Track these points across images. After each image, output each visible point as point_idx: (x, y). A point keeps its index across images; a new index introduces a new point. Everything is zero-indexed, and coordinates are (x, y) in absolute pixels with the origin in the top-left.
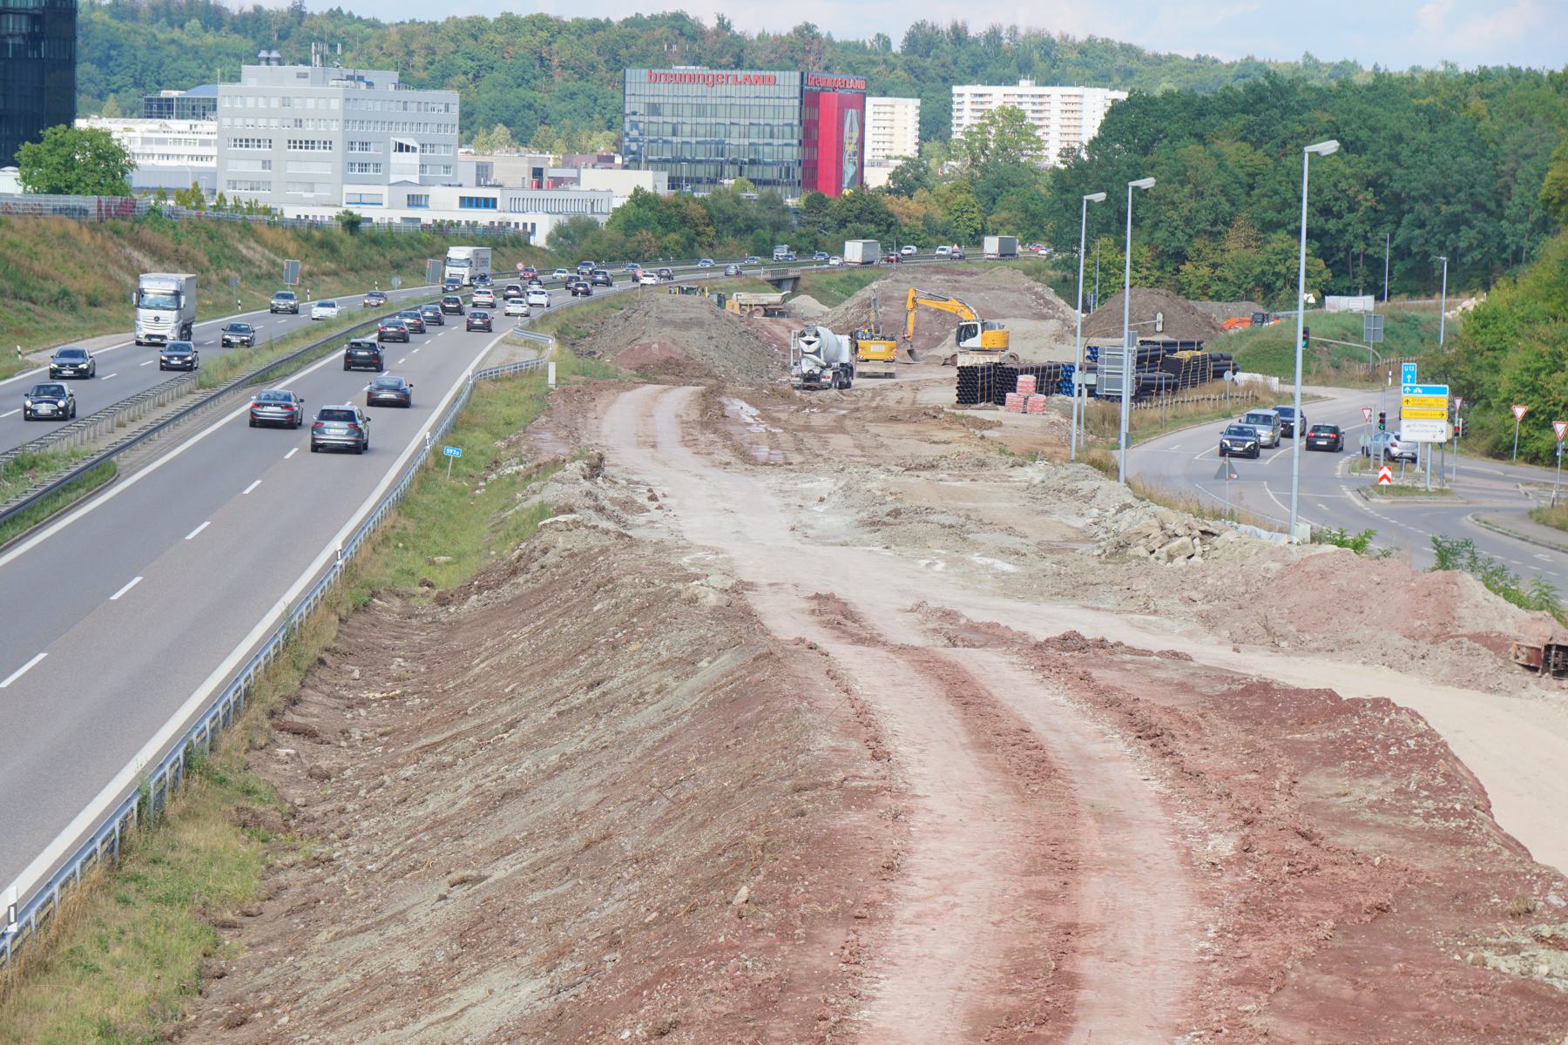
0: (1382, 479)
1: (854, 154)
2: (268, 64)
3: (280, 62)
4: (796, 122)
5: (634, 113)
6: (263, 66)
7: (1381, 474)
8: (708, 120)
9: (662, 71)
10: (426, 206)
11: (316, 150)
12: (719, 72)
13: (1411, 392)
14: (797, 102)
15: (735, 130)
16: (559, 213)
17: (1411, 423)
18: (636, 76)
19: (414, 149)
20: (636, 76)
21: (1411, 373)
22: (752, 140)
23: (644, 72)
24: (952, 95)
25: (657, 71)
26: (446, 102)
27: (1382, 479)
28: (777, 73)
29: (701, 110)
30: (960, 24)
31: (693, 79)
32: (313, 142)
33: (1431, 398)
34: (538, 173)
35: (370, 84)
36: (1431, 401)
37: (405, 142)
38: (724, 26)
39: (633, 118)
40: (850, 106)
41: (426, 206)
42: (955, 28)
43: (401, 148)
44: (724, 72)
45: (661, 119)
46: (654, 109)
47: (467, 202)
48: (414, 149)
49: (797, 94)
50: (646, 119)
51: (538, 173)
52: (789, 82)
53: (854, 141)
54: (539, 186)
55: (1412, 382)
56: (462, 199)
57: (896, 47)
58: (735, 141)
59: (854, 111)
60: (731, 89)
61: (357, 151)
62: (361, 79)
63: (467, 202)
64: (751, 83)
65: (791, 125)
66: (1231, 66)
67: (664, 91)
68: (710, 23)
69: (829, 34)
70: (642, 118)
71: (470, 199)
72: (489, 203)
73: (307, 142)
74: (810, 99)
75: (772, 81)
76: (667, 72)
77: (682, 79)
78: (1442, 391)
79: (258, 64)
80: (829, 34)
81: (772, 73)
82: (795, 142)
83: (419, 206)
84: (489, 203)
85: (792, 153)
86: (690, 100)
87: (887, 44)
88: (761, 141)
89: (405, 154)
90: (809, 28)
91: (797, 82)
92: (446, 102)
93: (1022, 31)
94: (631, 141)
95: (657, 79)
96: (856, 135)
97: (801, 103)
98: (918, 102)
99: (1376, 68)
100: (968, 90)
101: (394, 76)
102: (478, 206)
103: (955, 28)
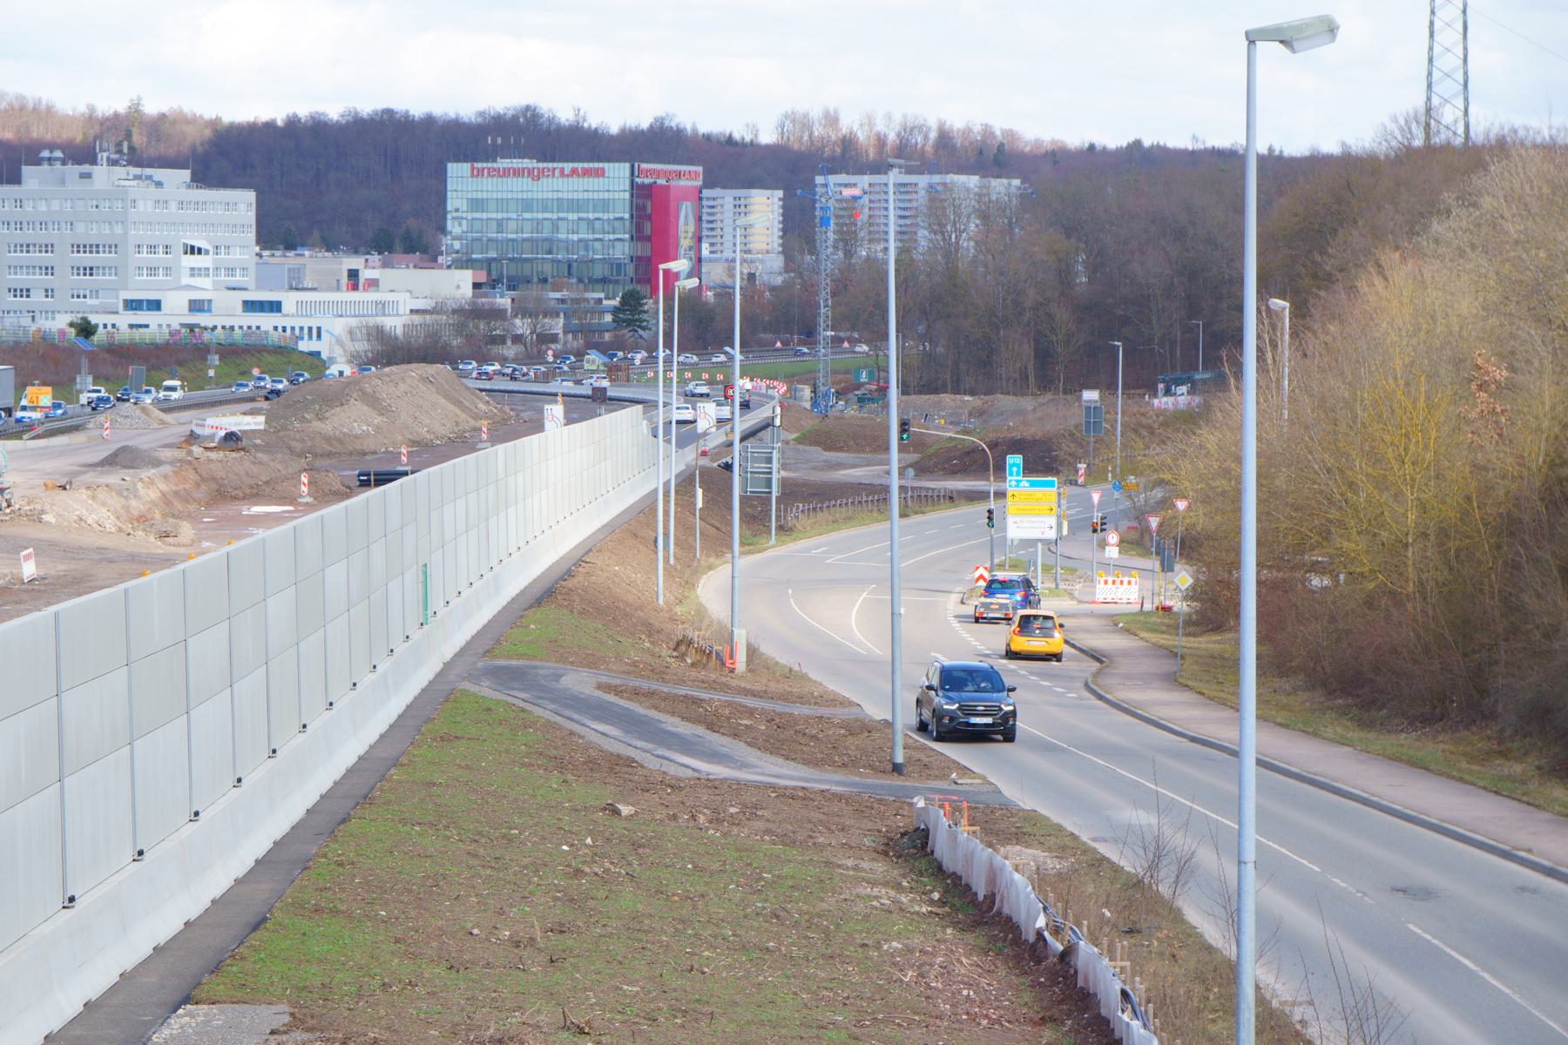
0: (977, 580)
1: (690, 248)
2: (50, 165)
3: (64, 163)
4: (627, 216)
5: (457, 210)
6: (45, 167)
7: (977, 574)
8: (535, 215)
9: (485, 165)
10: (209, 310)
11: (101, 255)
12: (545, 165)
13: (1017, 486)
14: (627, 195)
15: (562, 225)
16: (359, 316)
17: (1018, 519)
18: (457, 172)
19: (207, 252)
20: (457, 172)
21: (1014, 465)
22: (581, 236)
23: (466, 166)
24: (816, 186)
25: (479, 165)
26: (241, 204)
27: (977, 580)
28: (606, 165)
29: (527, 205)
30: (832, 112)
31: (518, 173)
32: (97, 246)
33: (1039, 492)
34: (353, 274)
35: (159, 184)
36: (1039, 495)
37: (197, 244)
39: (455, 214)
40: (686, 199)
41: (209, 310)
42: (827, 115)
43: (192, 250)
44: (550, 165)
45: (484, 216)
46: (476, 204)
47: (250, 306)
48: (207, 252)
49: (627, 187)
50: (470, 216)
51: (353, 274)
53: (690, 235)
54: (355, 287)
55: (1018, 475)
56: (246, 303)
58: (562, 236)
59: (689, 204)
61: (145, 255)
62: (149, 178)
63: (250, 306)
64: (578, 176)
65: (622, 219)
67: (489, 187)
69: (694, 124)
70: (464, 215)
71: (253, 303)
72: (275, 307)
73: (91, 246)
75: (600, 173)
76: (490, 165)
77: (506, 173)
78: (1051, 484)
79: (39, 164)
80: (694, 124)
81: (601, 165)
82: (627, 236)
83: (201, 310)
84: (275, 307)
85: (622, 251)
86: (515, 196)
88: (591, 237)
89: (196, 257)
91: (627, 174)
92: (241, 204)
94: (454, 239)
95: (480, 172)
96: (691, 228)
97: (632, 196)
98: (780, 193)
99: (1271, 150)
101: (186, 174)
102: (262, 310)
103: (827, 115)
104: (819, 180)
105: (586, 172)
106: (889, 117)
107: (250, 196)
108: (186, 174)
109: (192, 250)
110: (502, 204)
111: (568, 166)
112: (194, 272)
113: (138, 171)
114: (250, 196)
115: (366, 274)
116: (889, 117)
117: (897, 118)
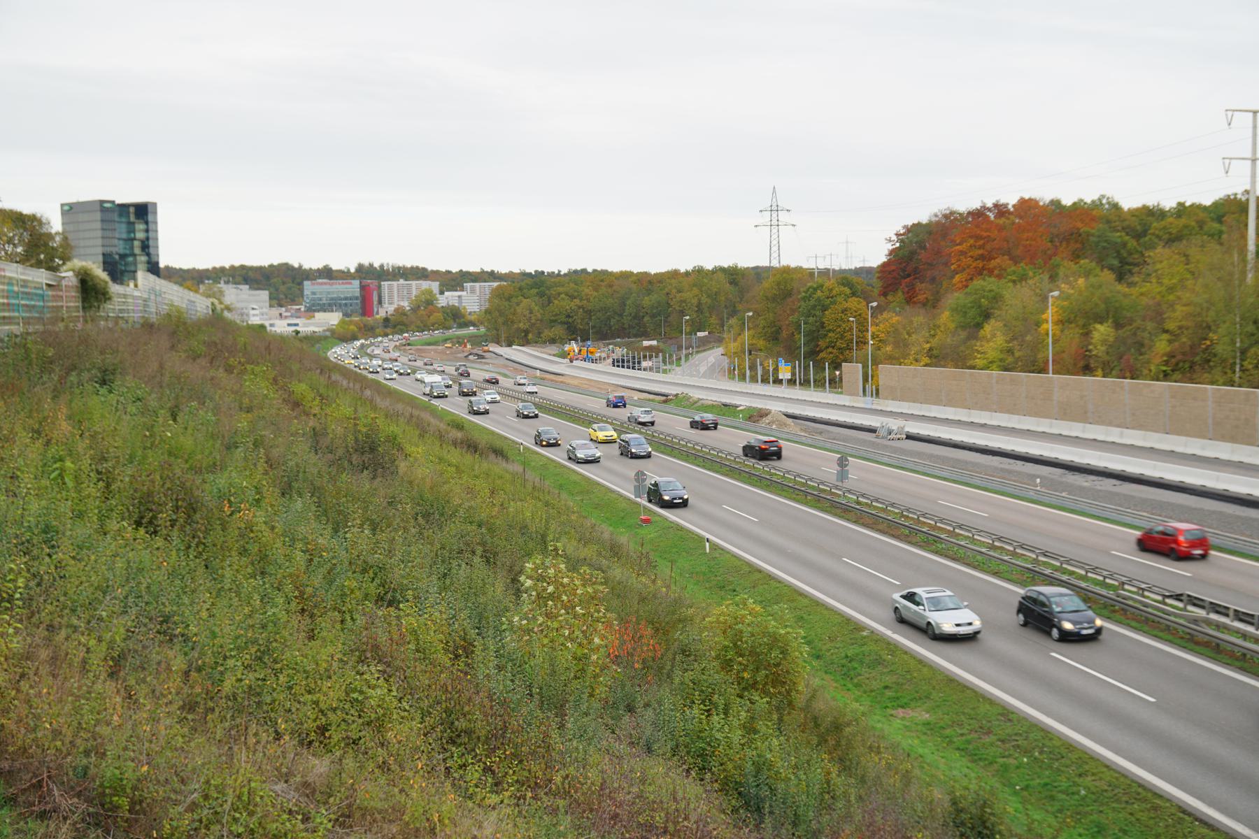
18: (307, 284)
20: (307, 284)
26: (264, 295)
29: (329, 293)
31: (325, 284)
34: (281, 314)
38: (300, 267)
43: (253, 309)
46: (314, 293)
51: (281, 314)
52: (356, 283)
57: (353, 270)
60: (338, 286)
66: (456, 273)
67: (317, 288)
68: (296, 265)
74: (363, 288)
75: (350, 283)
77: (322, 284)
87: (349, 270)
90: (327, 265)
92: (264, 295)
93: (390, 264)
100: (386, 283)
104: (465, 284)
105: (346, 283)
106: (388, 264)
107: (267, 293)
108: (247, 287)
109: (253, 309)
110: (321, 293)
111: (341, 281)
112: (254, 315)
113: (234, 286)
114: (267, 293)
115: (285, 314)
116: (388, 264)
117: (390, 264)
